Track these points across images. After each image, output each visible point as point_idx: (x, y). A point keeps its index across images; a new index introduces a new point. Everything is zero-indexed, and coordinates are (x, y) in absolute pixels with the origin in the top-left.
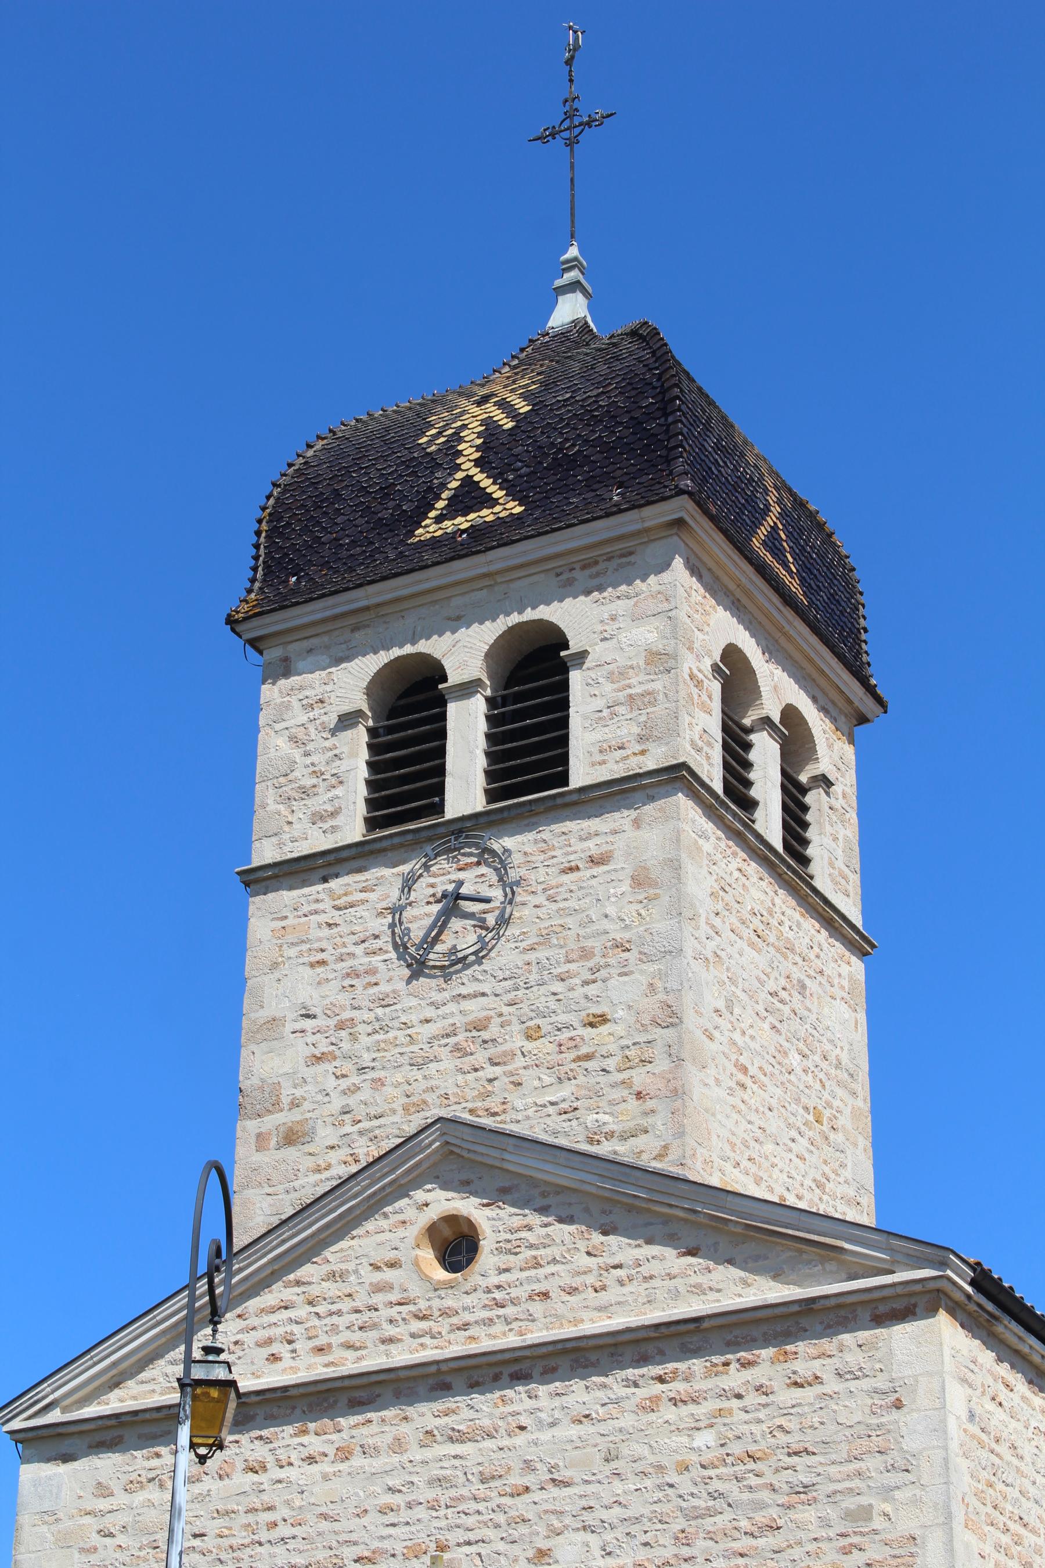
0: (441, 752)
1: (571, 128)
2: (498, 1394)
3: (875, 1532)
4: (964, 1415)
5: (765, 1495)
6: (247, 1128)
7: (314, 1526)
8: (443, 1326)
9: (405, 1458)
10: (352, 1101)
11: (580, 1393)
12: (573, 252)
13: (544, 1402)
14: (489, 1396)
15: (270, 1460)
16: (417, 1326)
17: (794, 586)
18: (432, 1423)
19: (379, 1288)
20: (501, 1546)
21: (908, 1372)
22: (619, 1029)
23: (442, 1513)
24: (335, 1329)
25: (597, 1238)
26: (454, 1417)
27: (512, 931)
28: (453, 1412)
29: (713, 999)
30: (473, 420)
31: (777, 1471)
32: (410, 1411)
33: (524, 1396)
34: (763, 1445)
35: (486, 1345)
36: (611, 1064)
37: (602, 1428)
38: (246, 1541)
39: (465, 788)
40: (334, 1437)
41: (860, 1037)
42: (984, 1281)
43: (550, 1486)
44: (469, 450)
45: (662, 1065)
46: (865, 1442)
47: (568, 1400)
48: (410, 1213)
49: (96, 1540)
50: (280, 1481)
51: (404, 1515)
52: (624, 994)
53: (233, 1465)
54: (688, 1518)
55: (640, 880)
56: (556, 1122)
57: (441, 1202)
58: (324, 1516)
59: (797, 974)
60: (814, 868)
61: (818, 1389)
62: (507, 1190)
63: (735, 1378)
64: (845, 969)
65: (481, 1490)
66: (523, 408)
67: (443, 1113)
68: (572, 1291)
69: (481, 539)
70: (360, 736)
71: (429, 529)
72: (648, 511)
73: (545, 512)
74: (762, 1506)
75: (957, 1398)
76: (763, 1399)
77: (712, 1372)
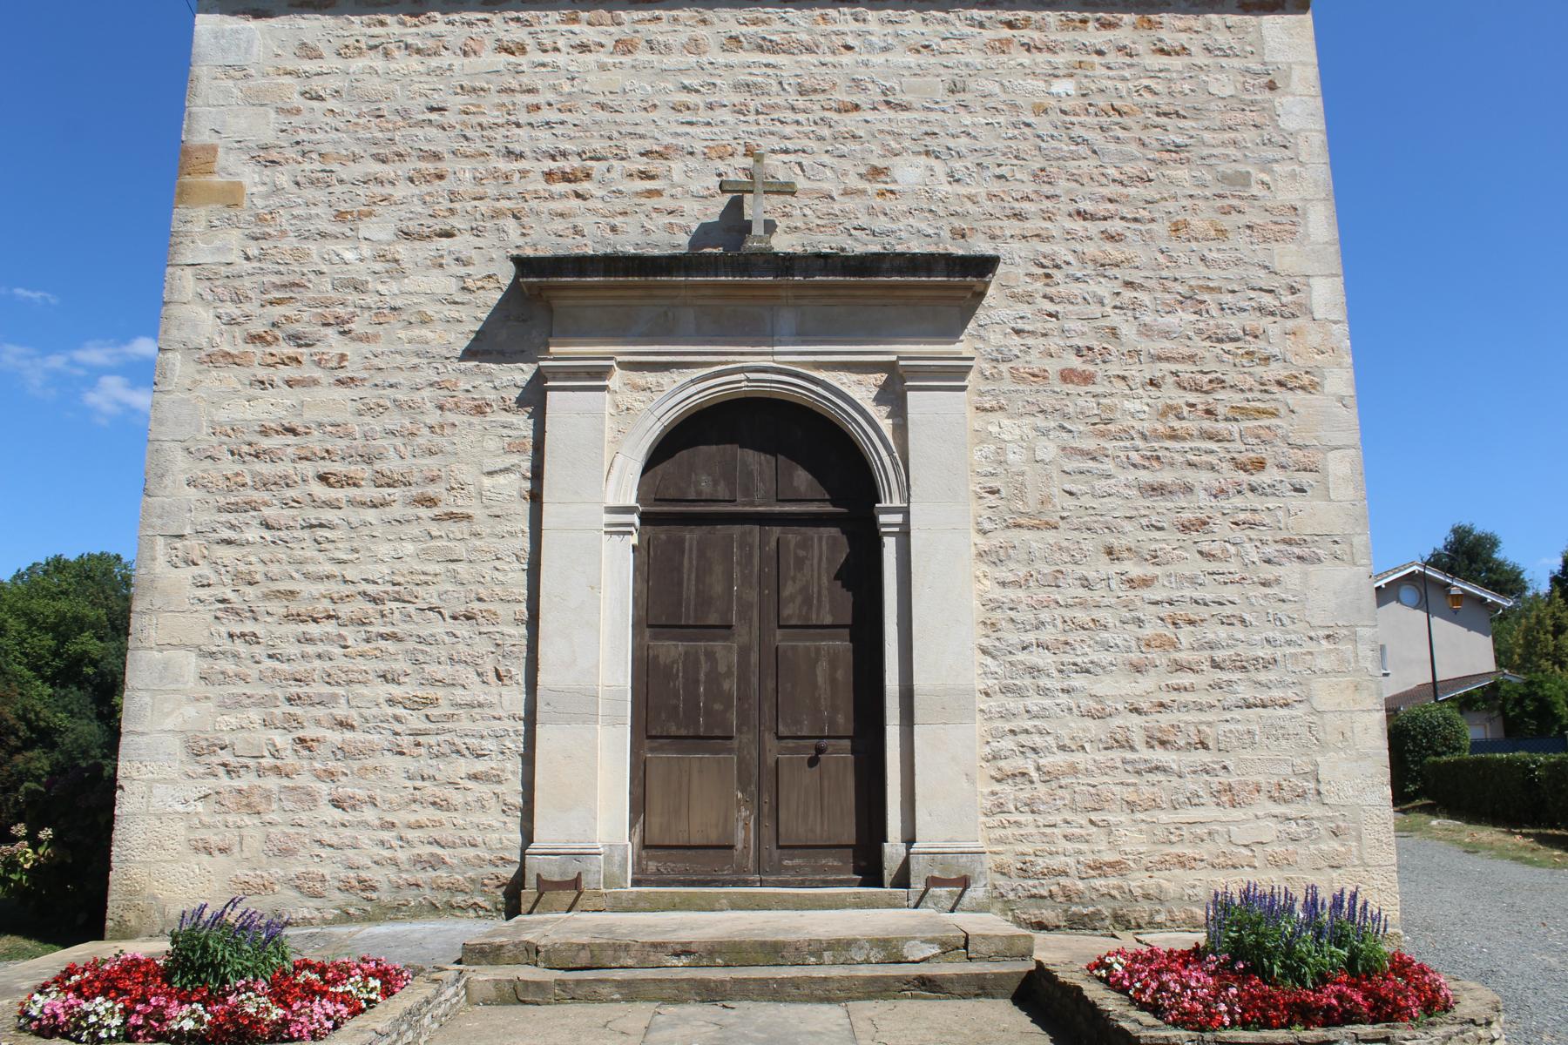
2: (818, 12)
3: (1254, 198)
9: (704, 59)
13: (873, 26)
14: (807, 12)
15: (530, 43)
18: (737, 30)
20: (826, 159)
21: (1280, 58)
23: (751, 118)
26: (764, 27)
28: (763, 22)
31: (1146, 127)
32: (708, 14)
33: (849, 17)
34: (1129, 101)
37: (944, 60)
38: (499, 121)
40: (612, 29)
43: (883, 108)
46: (1239, 115)
47: (905, 29)
49: (298, 101)
50: (544, 65)
51: (703, 116)
53: (481, 43)
54: (1047, 158)
58: (603, 107)
61: (1185, 59)
63: (1094, 36)
76: (1128, 60)
77: (1068, 25)
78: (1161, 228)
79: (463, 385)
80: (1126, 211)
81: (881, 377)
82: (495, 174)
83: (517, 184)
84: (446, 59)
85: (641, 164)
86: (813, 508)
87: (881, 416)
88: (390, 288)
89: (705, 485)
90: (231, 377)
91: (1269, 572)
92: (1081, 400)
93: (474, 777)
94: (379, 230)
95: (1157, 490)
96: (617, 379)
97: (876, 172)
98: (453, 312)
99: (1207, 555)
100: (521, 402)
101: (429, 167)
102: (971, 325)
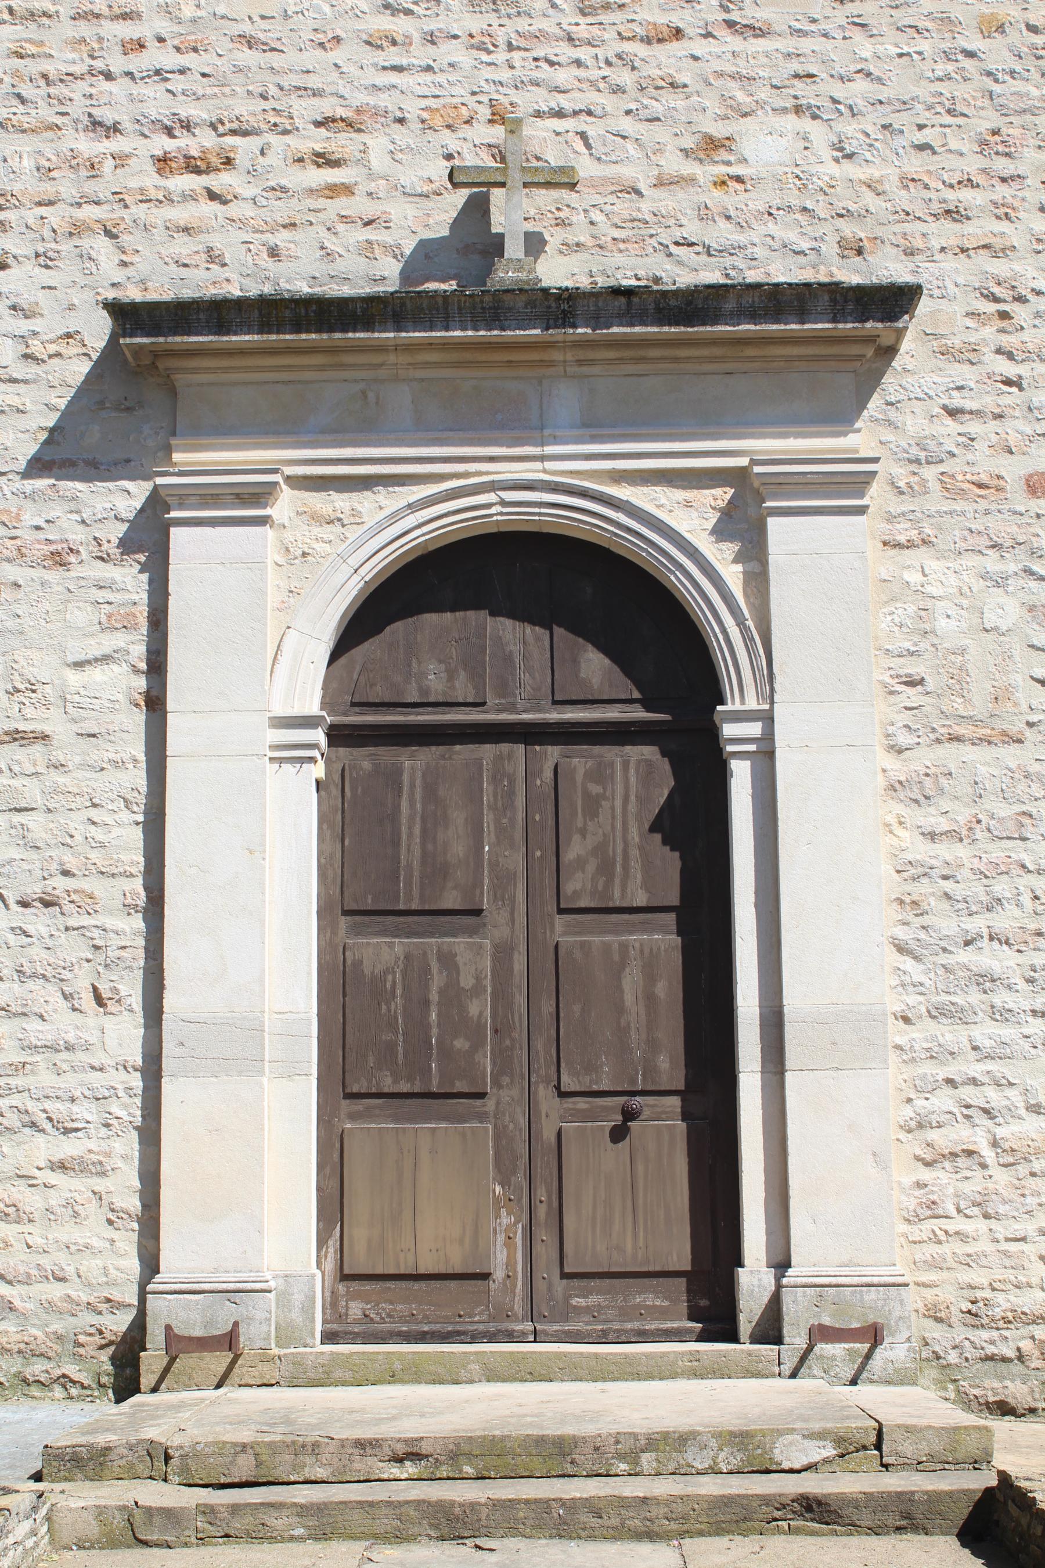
7: (222, 56)
20: (627, 125)
23: (501, 56)
38: (78, 69)
43: (722, 33)
51: (421, 54)
54: (1003, 111)
58: (250, 42)
79: (30, 518)
81: (723, 495)
82: (72, 161)
83: (111, 178)
85: (317, 140)
86: (613, 714)
89: (434, 679)
93: (62, 1166)
96: (285, 505)
100: (127, 546)
102: (875, 404)
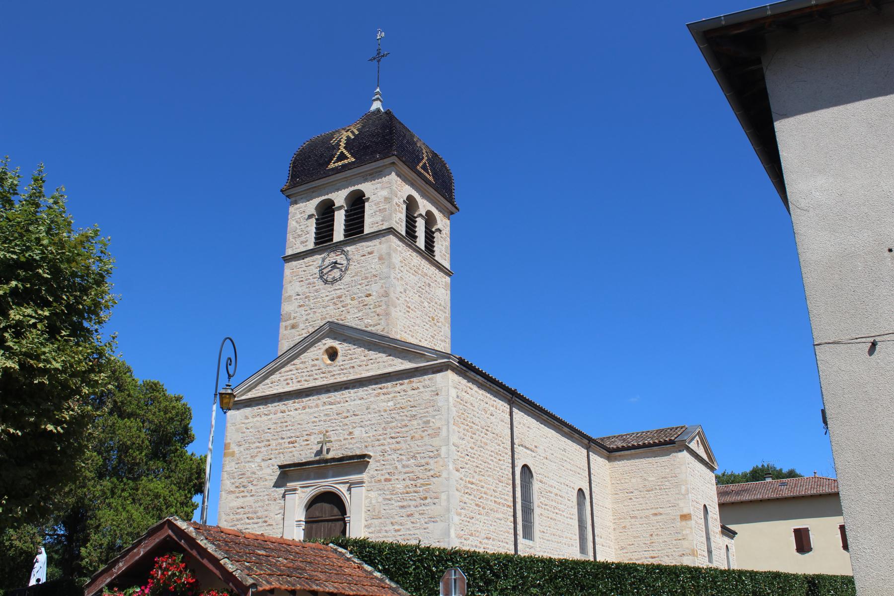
0: (333, 225)
1: (379, 57)
4: (455, 396)
5: (405, 418)
6: (283, 324)
8: (328, 375)
10: (308, 317)
11: (361, 392)
12: (378, 90)
16: (322, 375)
17: (431, 179)
19: (313, 366)
22: (374, 298)
24: (302, 376)
25: (367, 352)
27: (349, 272)
29: (400, 289)
30: (344, 135)
35: (339, 380)
36: (371, 307)
39: (339, 234)
41: (448, 298)
42: (461, 361)
44: (342, 144)
45: (384, 307)
48: (321, 346)
49: (245, 430)
51: (318, 424)
52: (375, 289)
55: (380, 258)
56: (358, 322)
57: (329, 343)
59: (427, 281)
60: (435, 253)
62: (345, 339)
63: (399, 388)
64: (444, 280)
65: (336, 417)
66: (357, 133)
67: (330, 320)
68: (360, 366)
69: (345, 168)
70: (313, 221)
71: (332, 166)
72: (385, 160)
73: (360, 160)
74: (403, 420)
75: (453, 393)
77: (393, 386)
78: (409, 439)
80: (401, 435)
84: (272, 416)
85: (306, 437)
87: (346, 494)
88: (260, 473)
89: (317, 514)
90: (233, 496)
91: (426, 526)
92: (388, 485)
94: (258, 459)
95: (402, 507)
97: (351, 433)
98: (271, 477)
99: (413, 523)
101: (267, 443)
